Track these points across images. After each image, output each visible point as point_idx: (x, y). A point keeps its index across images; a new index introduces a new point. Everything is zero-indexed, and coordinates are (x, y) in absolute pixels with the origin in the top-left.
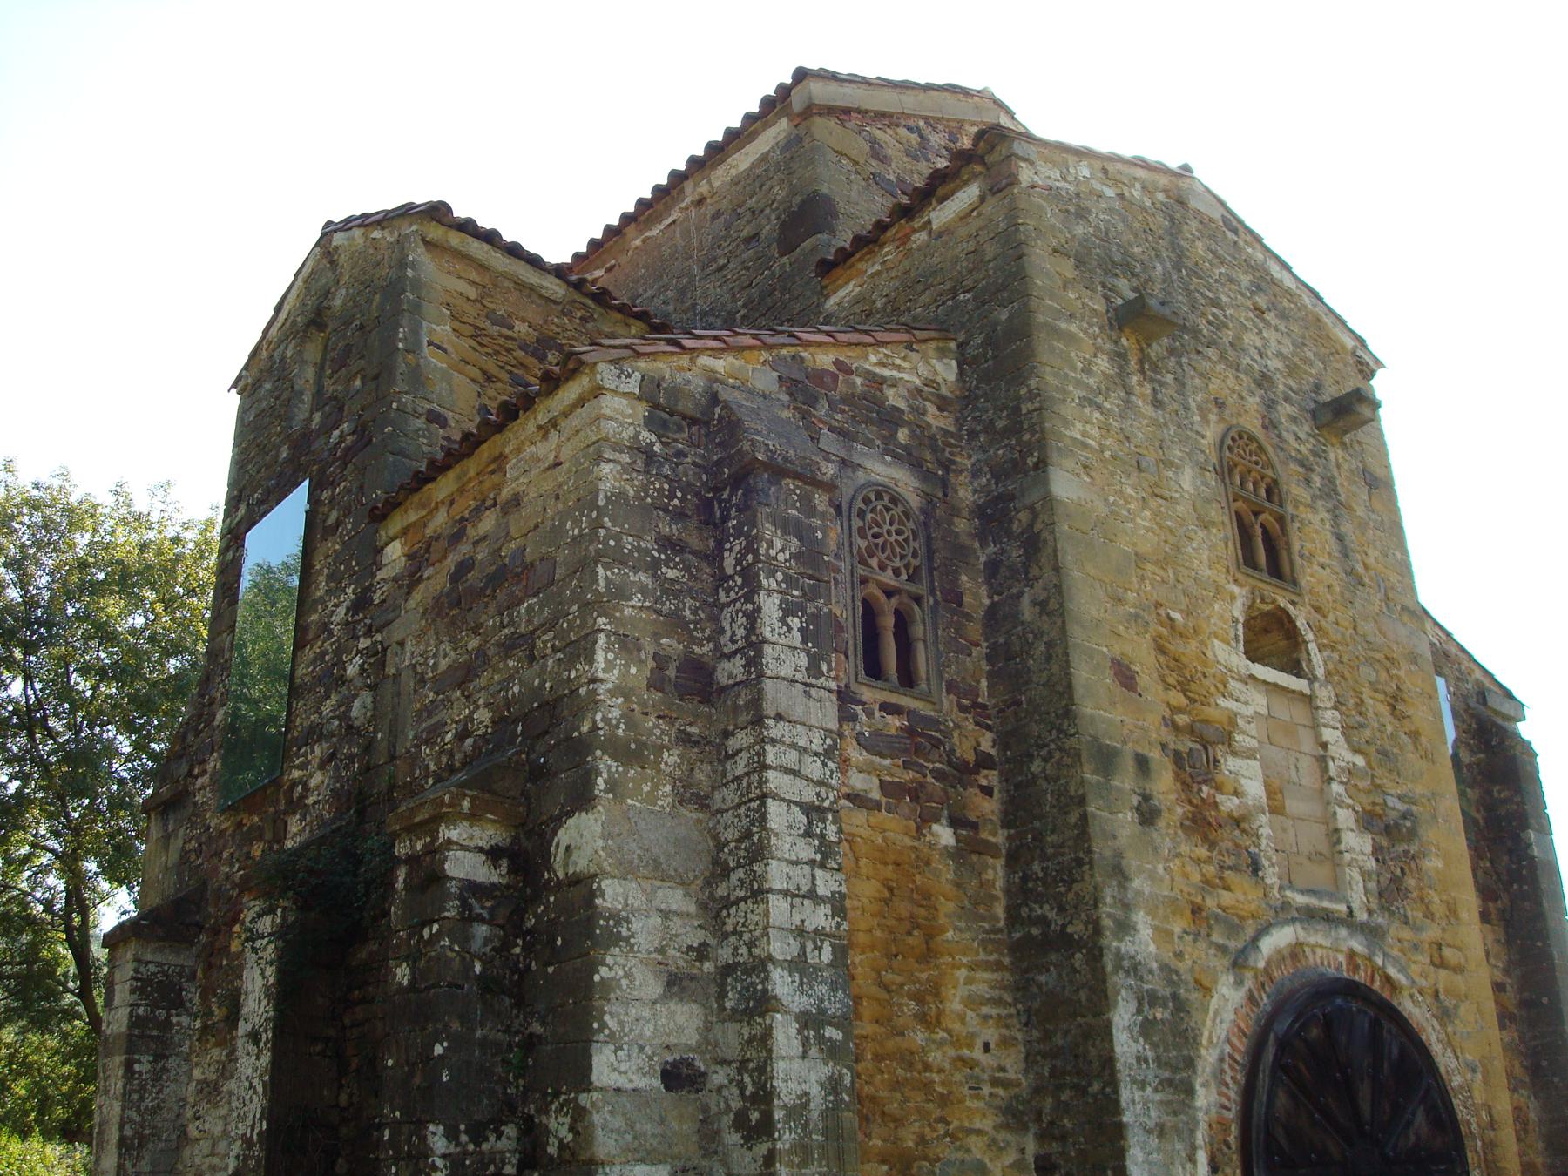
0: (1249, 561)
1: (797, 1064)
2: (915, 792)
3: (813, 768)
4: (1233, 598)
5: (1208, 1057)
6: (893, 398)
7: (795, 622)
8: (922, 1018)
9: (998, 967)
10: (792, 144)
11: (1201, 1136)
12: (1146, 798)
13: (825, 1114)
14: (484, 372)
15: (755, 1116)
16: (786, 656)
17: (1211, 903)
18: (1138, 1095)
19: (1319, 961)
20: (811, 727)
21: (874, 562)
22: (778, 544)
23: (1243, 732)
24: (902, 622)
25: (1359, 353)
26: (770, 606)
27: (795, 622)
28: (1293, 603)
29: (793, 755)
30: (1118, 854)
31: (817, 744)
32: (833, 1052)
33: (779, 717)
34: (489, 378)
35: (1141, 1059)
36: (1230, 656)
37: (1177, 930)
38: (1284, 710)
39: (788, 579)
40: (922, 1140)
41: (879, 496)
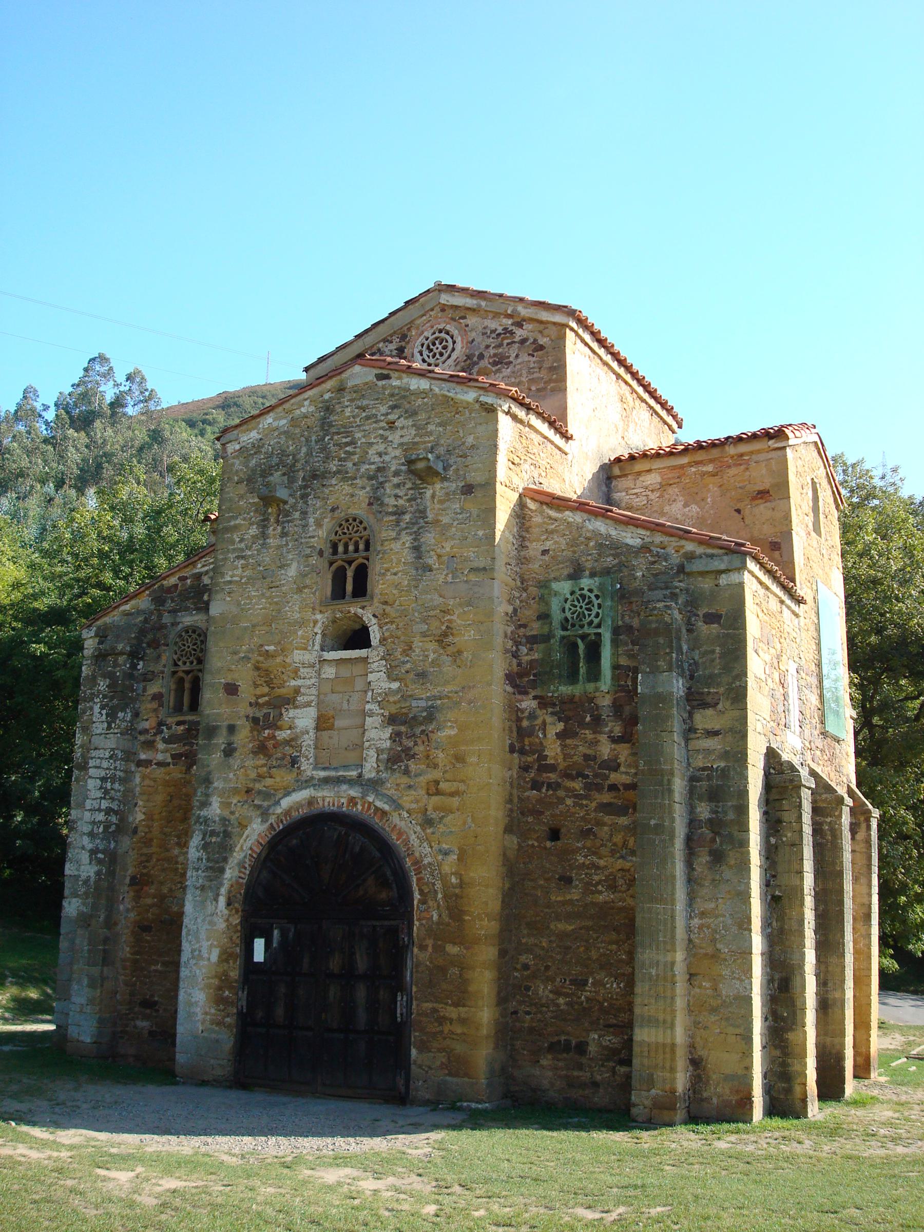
1: (88, 867)
3: (105, 764)
4: (315, 622)
5: (237, 856)
6: (206, 580)
7: (104, 712)
8: (178, 844)
11: (223, 891)
13: (95, 882)
18: (194, 874)
19: (326, 804)
20: (105, 749)
22: (102, 684)
23: (304, 695)
26: (97, 709)
27: (104, 712)
28: (363, 608)
29: (99, 761)
30: (209, 773)
31: (107, 755)
32: (100, 862)
33: (96, 749)
35: (200, 859)
37: (235, 801)
38: (345, 672)
39: (105, 697)
40: (171, 890)
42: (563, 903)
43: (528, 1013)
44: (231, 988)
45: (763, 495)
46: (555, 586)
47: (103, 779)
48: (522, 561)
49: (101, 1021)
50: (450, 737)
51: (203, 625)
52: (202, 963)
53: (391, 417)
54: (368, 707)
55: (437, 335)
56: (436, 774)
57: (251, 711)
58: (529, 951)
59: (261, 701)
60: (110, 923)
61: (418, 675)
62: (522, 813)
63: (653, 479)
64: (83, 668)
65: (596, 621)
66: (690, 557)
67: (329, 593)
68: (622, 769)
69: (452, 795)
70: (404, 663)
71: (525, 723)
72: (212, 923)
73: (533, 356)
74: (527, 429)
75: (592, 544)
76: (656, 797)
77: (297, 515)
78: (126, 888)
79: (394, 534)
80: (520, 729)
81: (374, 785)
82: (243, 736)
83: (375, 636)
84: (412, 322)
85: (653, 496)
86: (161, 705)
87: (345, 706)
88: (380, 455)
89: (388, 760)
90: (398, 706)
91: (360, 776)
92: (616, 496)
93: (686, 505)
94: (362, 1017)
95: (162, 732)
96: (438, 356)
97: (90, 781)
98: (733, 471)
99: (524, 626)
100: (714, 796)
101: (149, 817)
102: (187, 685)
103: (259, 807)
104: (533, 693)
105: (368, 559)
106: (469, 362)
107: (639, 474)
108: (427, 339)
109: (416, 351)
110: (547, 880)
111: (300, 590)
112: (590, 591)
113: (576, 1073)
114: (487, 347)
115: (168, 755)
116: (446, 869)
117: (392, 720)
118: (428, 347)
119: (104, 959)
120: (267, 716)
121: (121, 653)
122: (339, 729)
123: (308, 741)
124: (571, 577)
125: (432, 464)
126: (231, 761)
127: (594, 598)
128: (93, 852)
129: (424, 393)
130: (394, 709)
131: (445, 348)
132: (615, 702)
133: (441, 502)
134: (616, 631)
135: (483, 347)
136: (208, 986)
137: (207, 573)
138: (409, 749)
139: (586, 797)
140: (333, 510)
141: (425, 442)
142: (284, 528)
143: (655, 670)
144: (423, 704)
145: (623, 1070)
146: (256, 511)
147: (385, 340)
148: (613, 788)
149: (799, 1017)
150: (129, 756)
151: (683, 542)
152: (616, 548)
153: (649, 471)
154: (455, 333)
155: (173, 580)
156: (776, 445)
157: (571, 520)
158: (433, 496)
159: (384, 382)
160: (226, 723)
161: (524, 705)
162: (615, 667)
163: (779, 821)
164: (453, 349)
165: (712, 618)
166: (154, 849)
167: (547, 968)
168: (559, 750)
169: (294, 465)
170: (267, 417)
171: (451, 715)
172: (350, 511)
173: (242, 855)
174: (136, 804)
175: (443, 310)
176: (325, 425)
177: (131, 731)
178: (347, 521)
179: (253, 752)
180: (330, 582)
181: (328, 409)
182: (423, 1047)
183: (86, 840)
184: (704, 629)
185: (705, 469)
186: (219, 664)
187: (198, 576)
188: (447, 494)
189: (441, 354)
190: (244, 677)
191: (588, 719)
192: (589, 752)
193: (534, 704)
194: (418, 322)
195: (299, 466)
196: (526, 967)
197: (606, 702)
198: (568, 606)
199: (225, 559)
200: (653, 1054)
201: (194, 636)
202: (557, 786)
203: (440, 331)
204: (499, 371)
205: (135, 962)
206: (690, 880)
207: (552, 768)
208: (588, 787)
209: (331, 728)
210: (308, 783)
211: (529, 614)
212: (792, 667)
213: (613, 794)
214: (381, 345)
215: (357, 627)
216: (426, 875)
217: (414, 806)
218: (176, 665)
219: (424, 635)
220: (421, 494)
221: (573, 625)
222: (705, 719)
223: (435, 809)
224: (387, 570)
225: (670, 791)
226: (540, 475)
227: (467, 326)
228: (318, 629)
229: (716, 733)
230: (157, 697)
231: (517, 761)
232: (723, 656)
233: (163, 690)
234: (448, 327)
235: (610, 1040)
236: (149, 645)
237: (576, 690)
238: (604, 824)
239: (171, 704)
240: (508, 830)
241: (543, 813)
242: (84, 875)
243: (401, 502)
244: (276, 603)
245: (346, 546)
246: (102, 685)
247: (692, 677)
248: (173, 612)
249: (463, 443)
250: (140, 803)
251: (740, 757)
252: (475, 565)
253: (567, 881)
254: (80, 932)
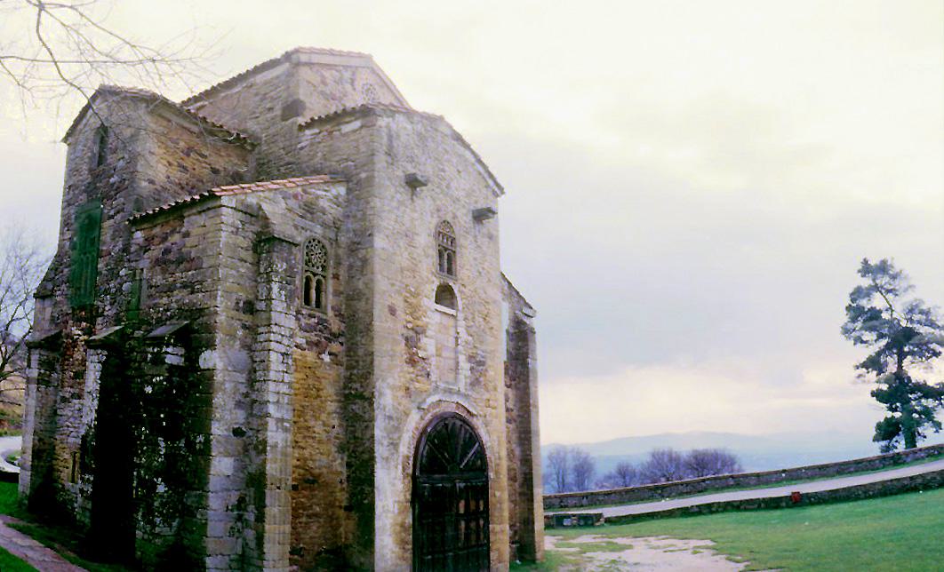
0: (442, 269)
2: (317, 344)
3: (286, 341)
9: (339, 401)
10: (290, 75)
13: (282, 448)
14: (168, 162)
15: (261, 447)
16: (280, 304)
17: (411, 387)
21: (310, 264)
26: (275, 287)
32: (286, 430)
34: (170, 164)
36: (429, 302)
38: (445, 320)
40: (311, 455)
41: (314, 240)
47: (283, 354)
59: (410, 326)
64: (223, 234)
72: (394, 485)
83: (460, 303)
102: (314, 284)
115: (304, 341)
178: (444, 222)
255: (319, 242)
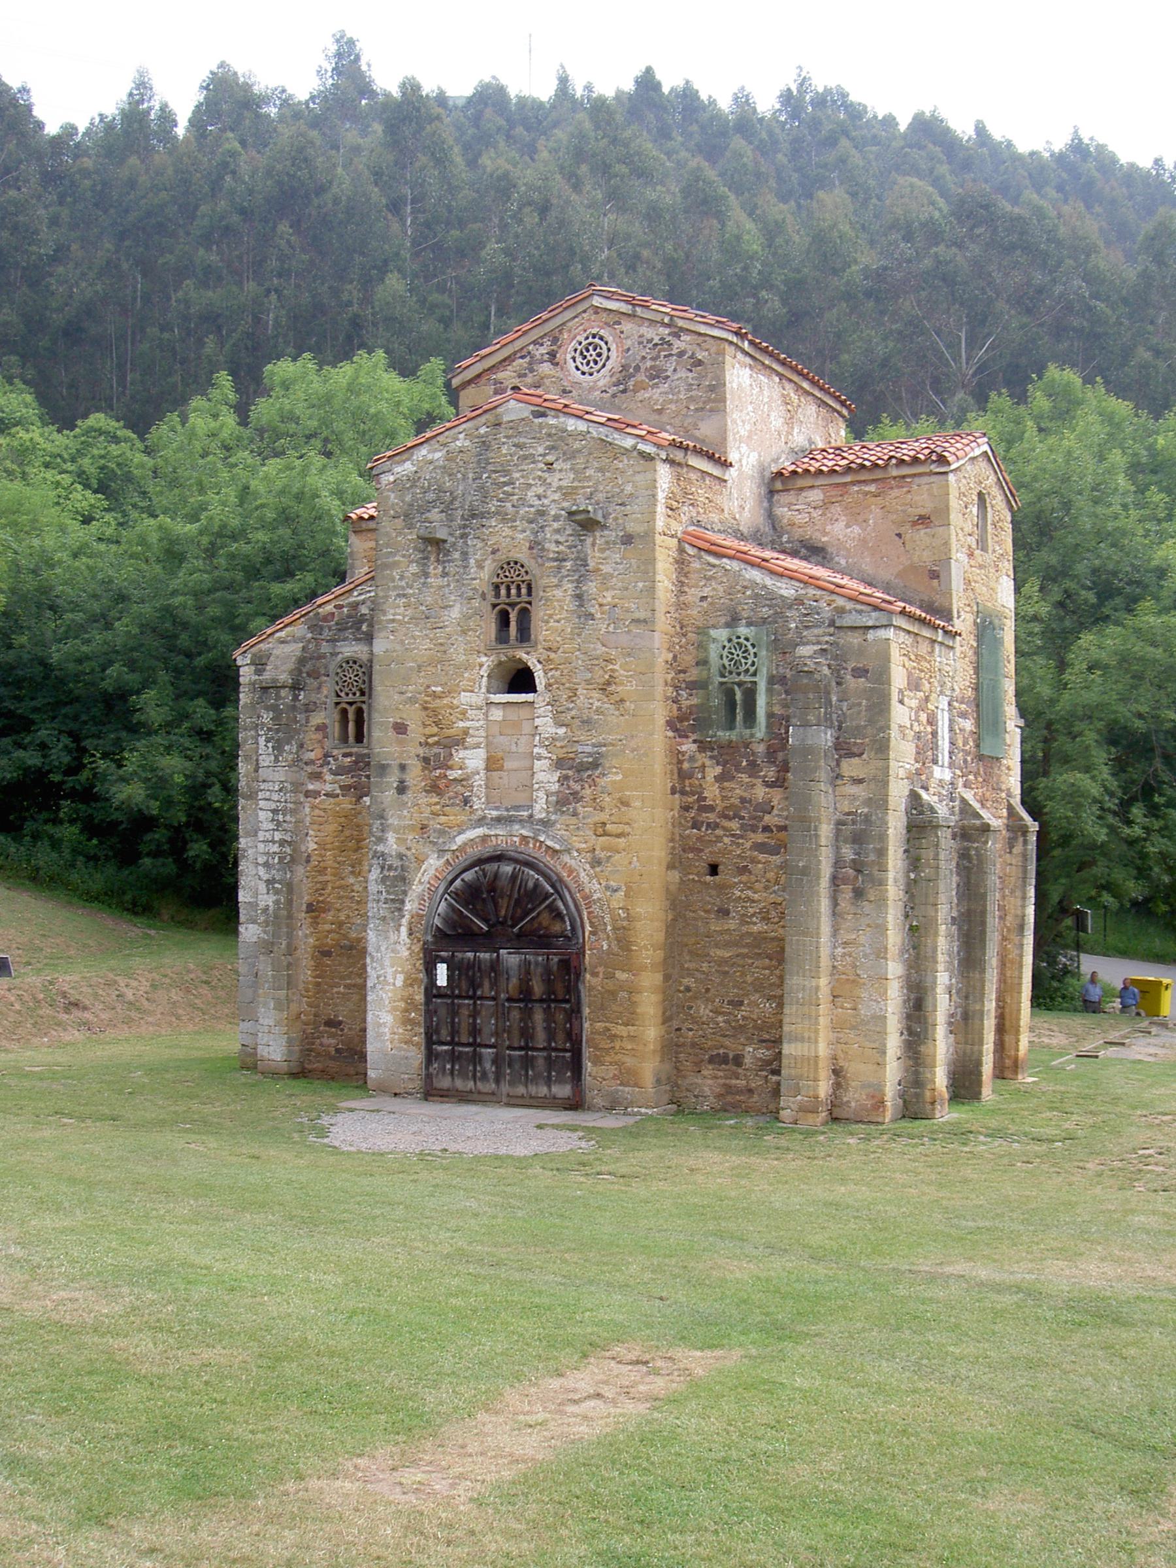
3: (275, 797)
4: (481, 666)
6: (364, 610)
7: (270, 745)
8: (352, 873)
11: (404, 921)
12: (402, 782)
24: (359, 712)
25: (640, 446)
26: (262, 741)
27: (270, 745)
28: (528, 653)
31: (277, 788)
32: (277, 892)
37: (410, 837)
38: (513, 715)
39: (269, 729)
40: (348, 917)
41: (348, 662)
42: (721, 933)
43: (691, 1030)
44: (416, 1009)
45: (923, 520)
46: (713, 633)
47: (275, 811)
48: (681, 606)
49: (290, 1042)
50: (614, 782)
51: (364, 657)
52: (387, 988)
53: (550, 458)
54: (536, 750)
55: (590, 340)
56: (603, 816)
57: (421, 751)
58: (690, 975)
59: (430, 740)
60: (291, 950)
61: (583, 722)
62: (684, 851)
63: (815, 496)
64: (241, 696)
65: (752, 669)
66: (841, 611)
67: (493, 636)
68: (775, 812)
69: (618, 836)
70: (571, 709)
71: (686, 765)
73: (691, 371)
74: (685, 470)
75: (748, 593)
76: (804, 842)
77: (457, 555)
78: (303, 915)
79: (555, 581)
80: (680, 770)
81: (546, 823)
82: (415, 776)
84: (564, 324)
85: (816, 514)
86: (326, 737)
87: (514, 748)
88: (539, 497)
89: (557, 802)
90: (565, 750)
91: (531, 816)
92: (781, 511)
93: (848, 526)
94: (541, 1038)
95: (329, 763)
96: (592, 364)
97: (261, 813)
98: (895, 493)
99: (684, 672)
100: (858, 839)
101: (322, 846)
103: (435, 844)
104: (694, 737)
105: (530, 603)
106: (624, 373)
107: (801, 489)
108: (580, 343)
109: (569, 356)
110: (707, 912)
111: (464, 632)
112: (747, 639)
113: (734, 1082)
114: (644, 358)
116: (614, 904)
117: (559, 764)
118: (582, 353)
119: (288, 983)
120: (437, 755)
121: (284, 687)
122: (508, 771)
123: (479, 781)
124: (728, 625)
125: (591, 515)
126: (404, 797)
127: (750, 647)
128: (269, 882)
129: (583, 435)
130: (561, 753)
131: (599, 355)
132: (769, 747)
133: (602, 551)
134: (771, 680)
135: (639, 358)
136: (395, 1009)
137: (363, 602)
138: (576, 793)
139: (741, 837)
140: (493, 552)
141: (584, 487)
142: (445, 568)
143: (806, 725)
144: (589, 749)
145: (775, 1078)
146: (415, 549)
147: (535, 342)
148: (766, 829)
149: (930, 1032)
150: (297, 787)
151: (834, 597)
152: (771, 598)
153: (812, 487)
154: (610, 339)
155: (329, 608)
156: (938, 470)
157: (728, 567)
158: (593, 545)
159: (540, 420)
160: (398, 761)
161: (684, 748)
162: (770, 715)
163: (918, 859)
164: (608, 358)
165: (860, 672)
166: (328, 878)
167: (708, 990)
168: (717, 792)
169: (451, 502)
170: (421, 448)
171: (614, 762)
172: (511, 554)
173: (421, 888)
174: (307, 834)
175: (596, 313)
176: (483, 462)
177: (297, 762)
179: (426, 791)
180: (493, 625)
181: (485, 445)
182: (597, 1061)
183: (262, 871)
184: (851, 682)
185: (867, 489)
186: (386, 703)
187: (355, 606)
188: (607, 543)
189: (596, 362)
190: (414, 718)
191: (744, 763)
192: (745, 795)
193: (694, 747)
194: (570, 324)
195: (457, 504)
196: (688, 989)
197: (761, 749)
198: (725, 653)
199: (387, 597)
200: (799, 1066)
201: (356, 667)
202: (717, 826)
203: (594, 336)
204: (656, 386)
205: (318, 984)
206: (835, 914)
207: (711, 809)
208: (742, 827)
209: (501, 769)
210: (481, 822)
211: (688, 659)
212: (943, 703)
213: (767, 834)
214: (531, 347)
215: (521, 666)
216: (596, 908)
217: (584, 846)
218: (338, 696)
219: (589, 682)
220: (581, 541)
221: (731, 673)
222: (851, 767)
223: (603, 849)
224: (551, 616)
225: (817, 836)
226: (698, 513)
227: (622, 332)
228: (484, 672)
229: (860, 781)
230: (321, 728)
231: (678, 802)
232: (869, 708)
233: (327, 721)
234: (602, 333)
235: (763, 1053)
236: (309, 675)
237: (733, 735)
238: (759, 862)
239: (336, 735)
240: (671, 866)
241: (702, 851)
242: (262, 904)
243: (561, 548)
244: (441, 644)
245: (508, 589)
246: (266, 717)
247: (840, 728)
248: (332, 641)
249: (622, 491)
250: (311, 832)
251: (880, 802)
252: (637, 615)
253: (726, 913)
254: (262, 958)
255: (355, 662)
